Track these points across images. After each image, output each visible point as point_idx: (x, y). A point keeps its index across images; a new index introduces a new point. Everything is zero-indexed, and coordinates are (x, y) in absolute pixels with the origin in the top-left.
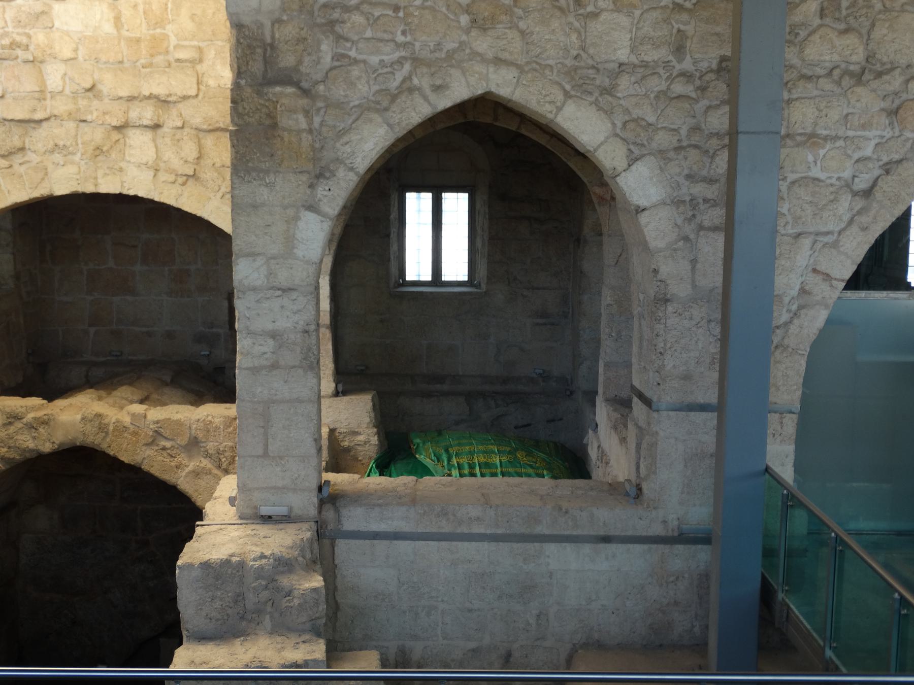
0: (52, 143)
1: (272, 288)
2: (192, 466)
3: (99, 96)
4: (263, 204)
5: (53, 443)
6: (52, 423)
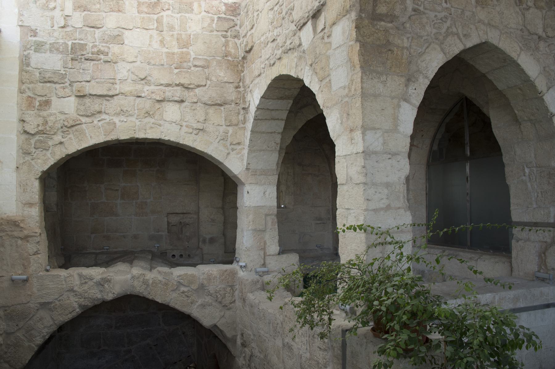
0: (119, 109)
1: (386, 153)
2: (200, 302)
3: (148, 83)
4: (379, 95)
5: (114, 293)
6: (112, 281)
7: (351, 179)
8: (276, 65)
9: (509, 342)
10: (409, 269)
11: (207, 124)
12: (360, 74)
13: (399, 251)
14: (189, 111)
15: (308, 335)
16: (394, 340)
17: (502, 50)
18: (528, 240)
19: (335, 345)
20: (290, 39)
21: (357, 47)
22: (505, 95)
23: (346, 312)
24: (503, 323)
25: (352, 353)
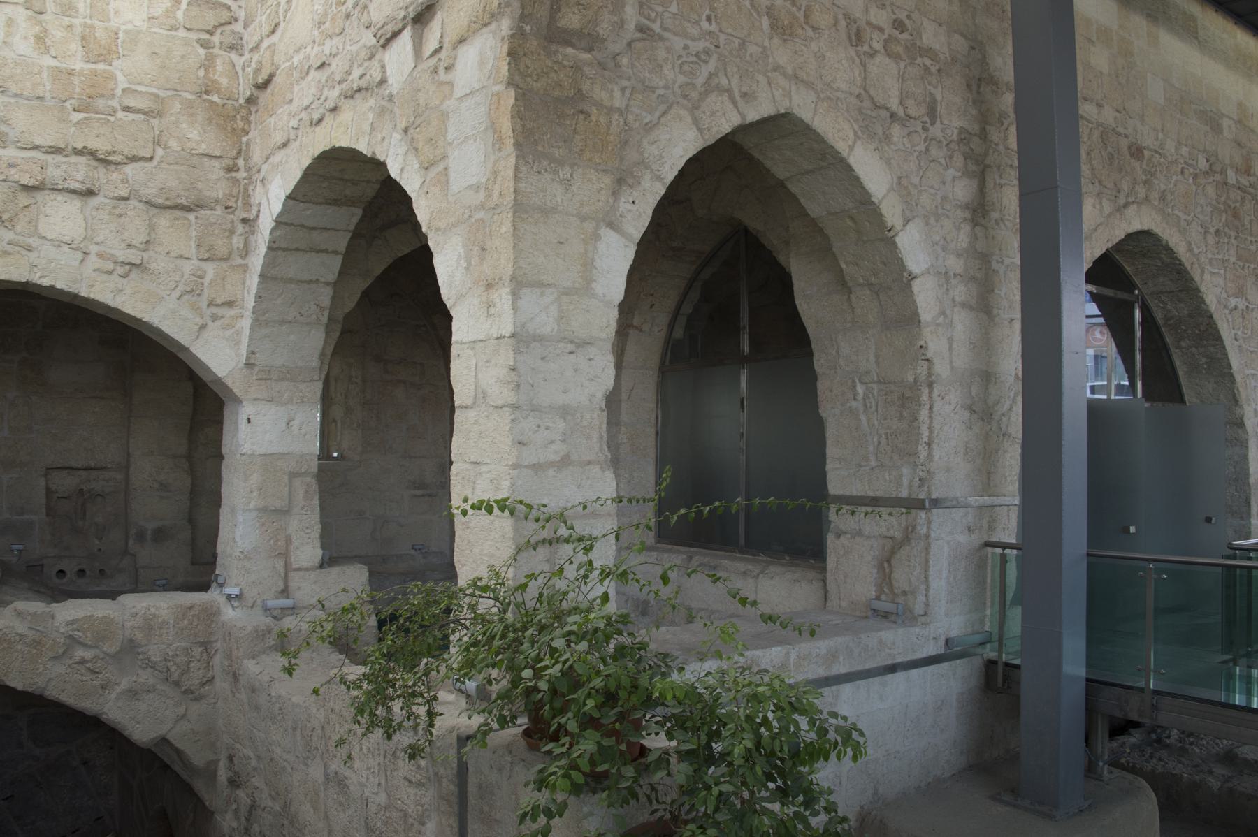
1: (563, 339)
2: (124, 684)
4: (554, 210)
7: (485, 394)
8: (324, 124)
9: (806, 747)
10: (605, 598)
11: (151, 253)
12: (513, 160)
13: (585, 558)
14: (106, 218)
15: (382, 752)
16: (568, 754)
17: (819, 135)
18: (859, 533)
19: (442, 771)
20: (360, 65)
21: (510, 98)
22: (821, 230)
23: (468, 696)
24: (794, 708)
25: (480, 787)
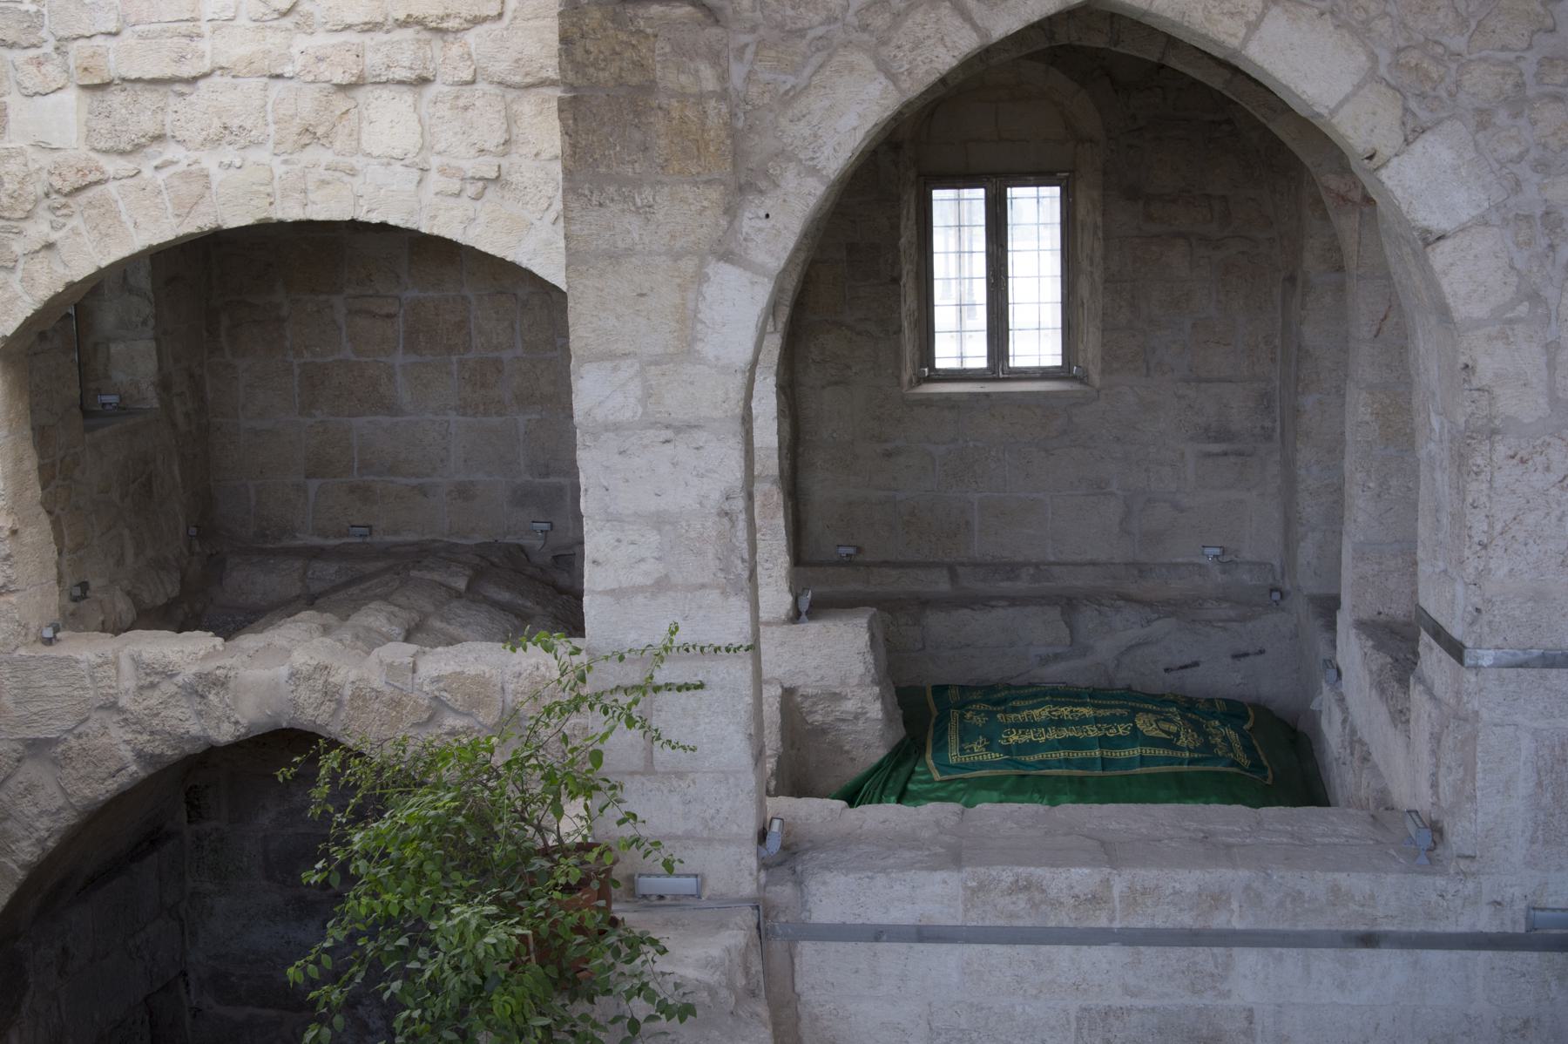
0: (217, 123)
1: (654, 425)
3: (306, 26)
4: (629, 252)
5: (237, 723)
6: (231, 685)
11: (515, 158)
14: (448, 114)
